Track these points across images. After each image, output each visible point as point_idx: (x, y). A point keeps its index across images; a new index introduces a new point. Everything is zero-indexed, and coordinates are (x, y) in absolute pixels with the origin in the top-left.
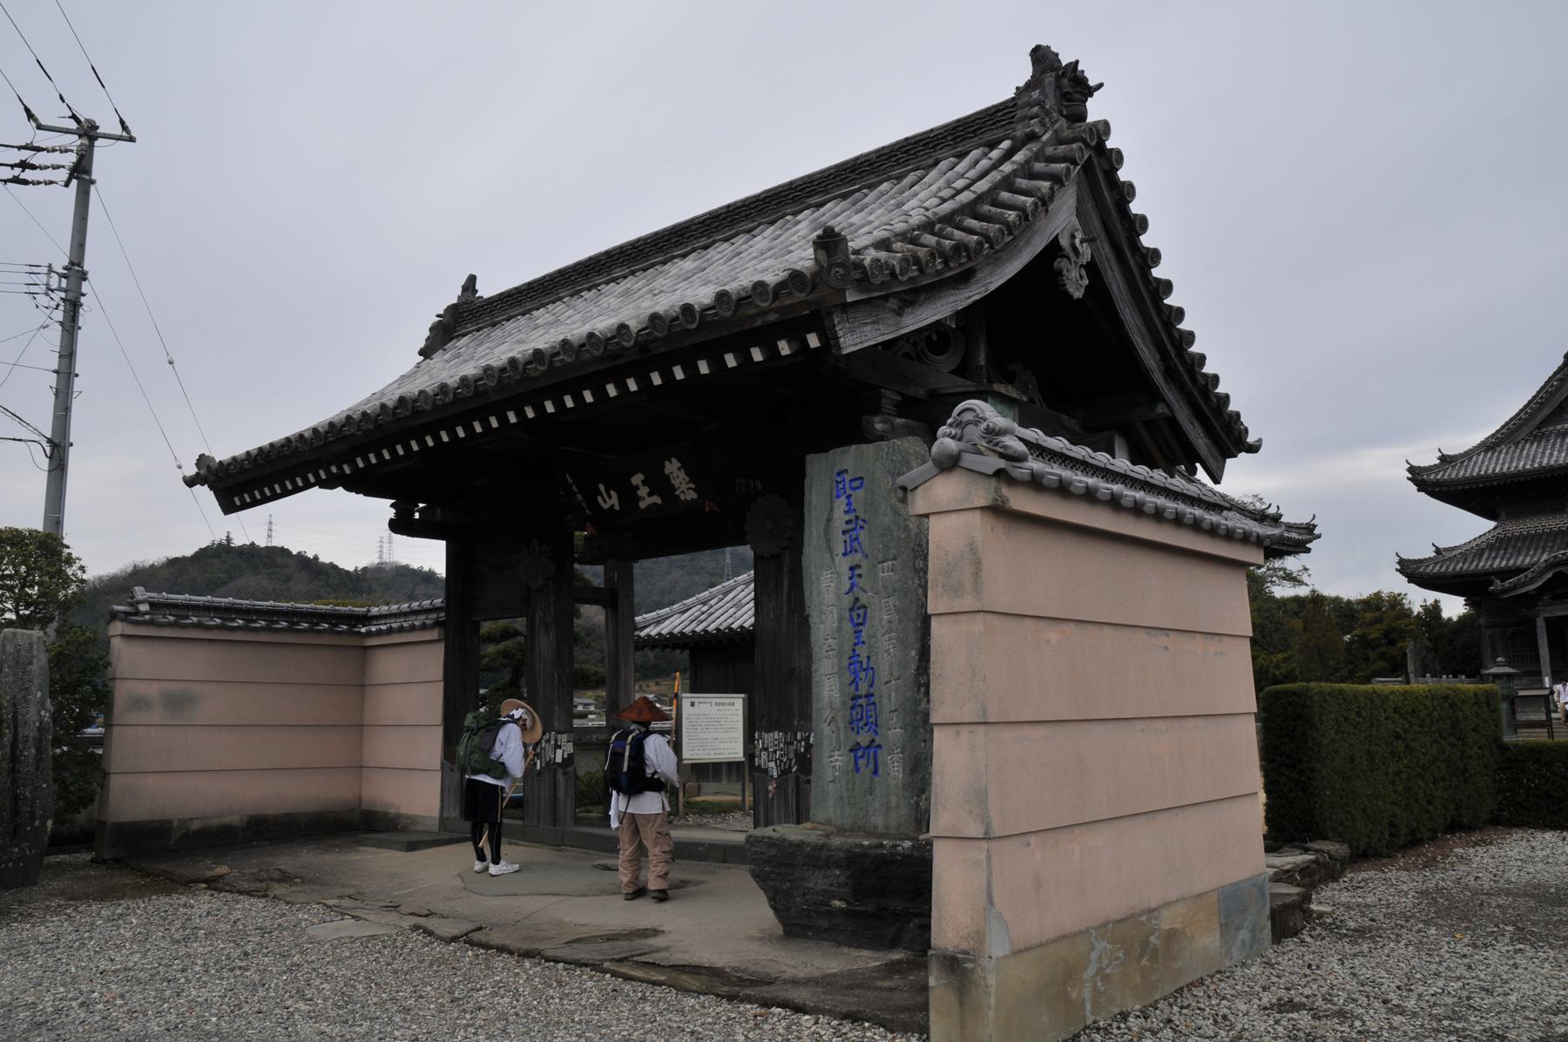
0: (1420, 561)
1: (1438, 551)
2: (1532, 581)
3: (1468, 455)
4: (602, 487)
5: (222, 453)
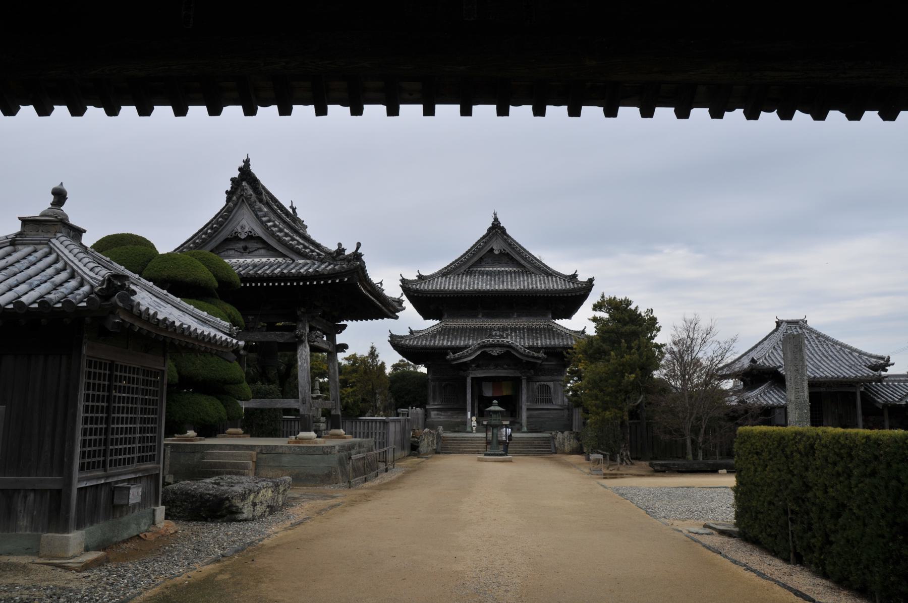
0: (402, 337)
1: (412, 332)
2: (470, 355)
3: (433, 277)
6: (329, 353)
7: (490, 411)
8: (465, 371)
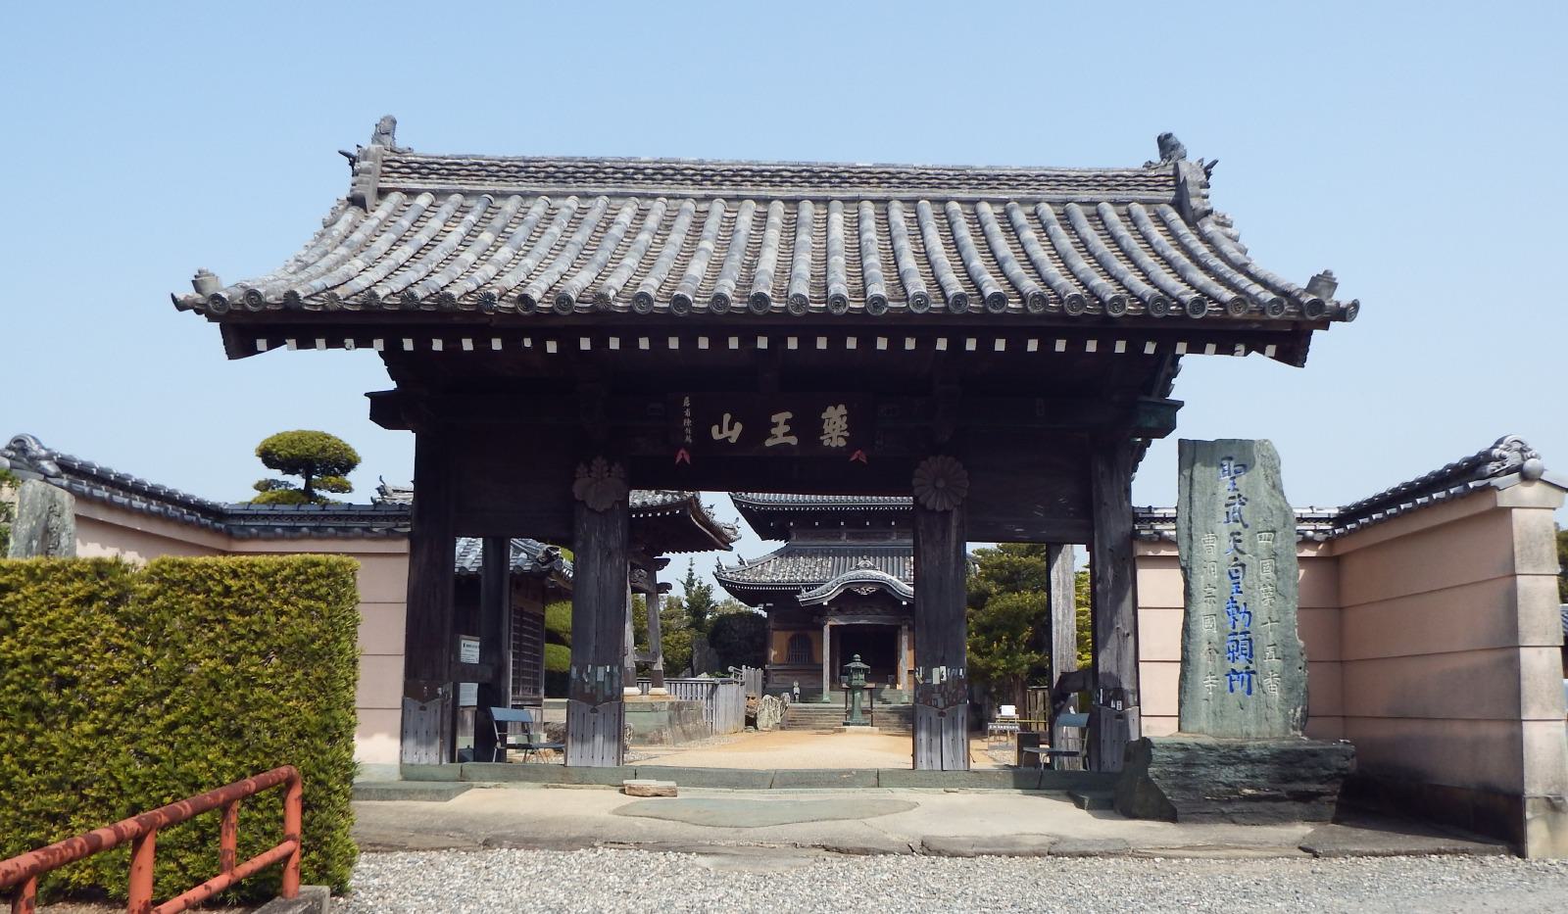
4: (727, 417)
5: (229, 282)
6: (649, 595)
7: (849, 668)
8: (820, 616)
